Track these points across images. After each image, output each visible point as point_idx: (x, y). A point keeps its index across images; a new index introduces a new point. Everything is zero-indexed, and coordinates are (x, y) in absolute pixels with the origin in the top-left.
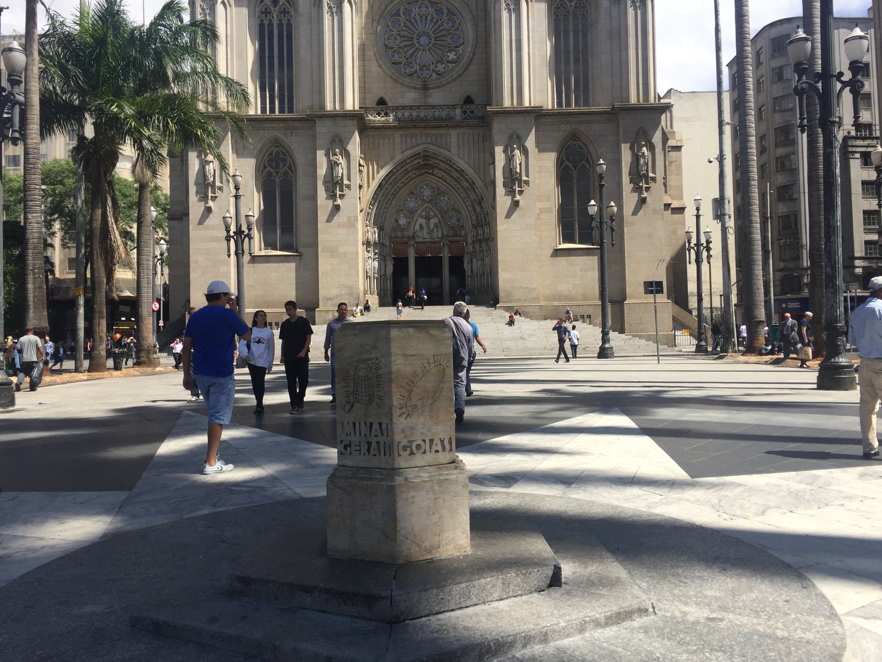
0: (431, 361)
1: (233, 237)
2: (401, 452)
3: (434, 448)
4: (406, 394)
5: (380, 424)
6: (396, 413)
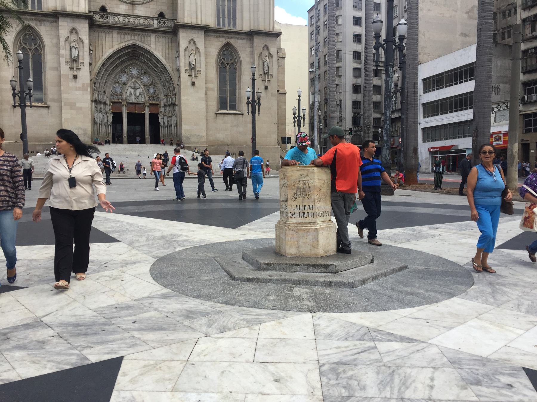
1: (17, 94)
5: (309, 206)
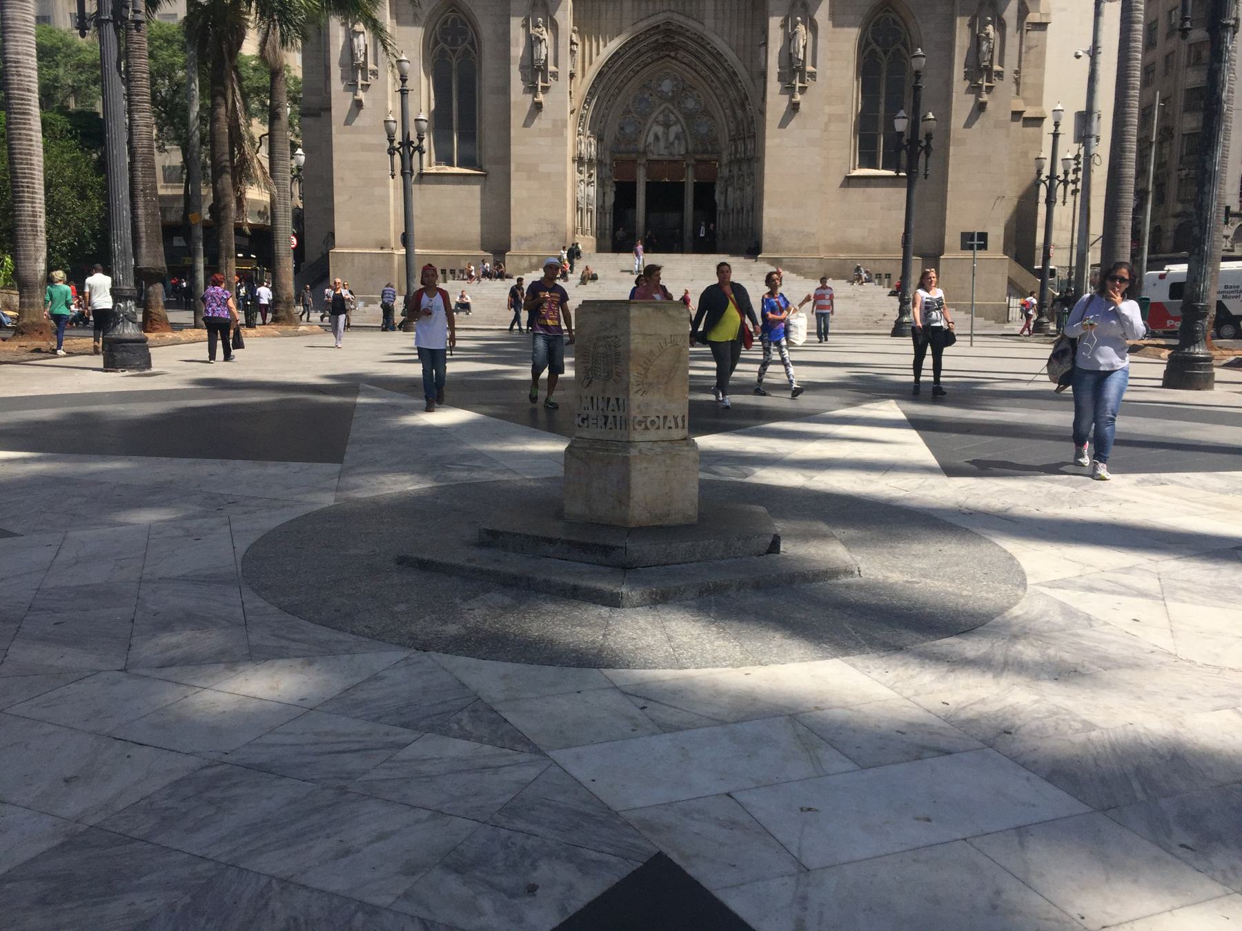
3: (668, 424)
5: (617, 400)
6: (633, 389)
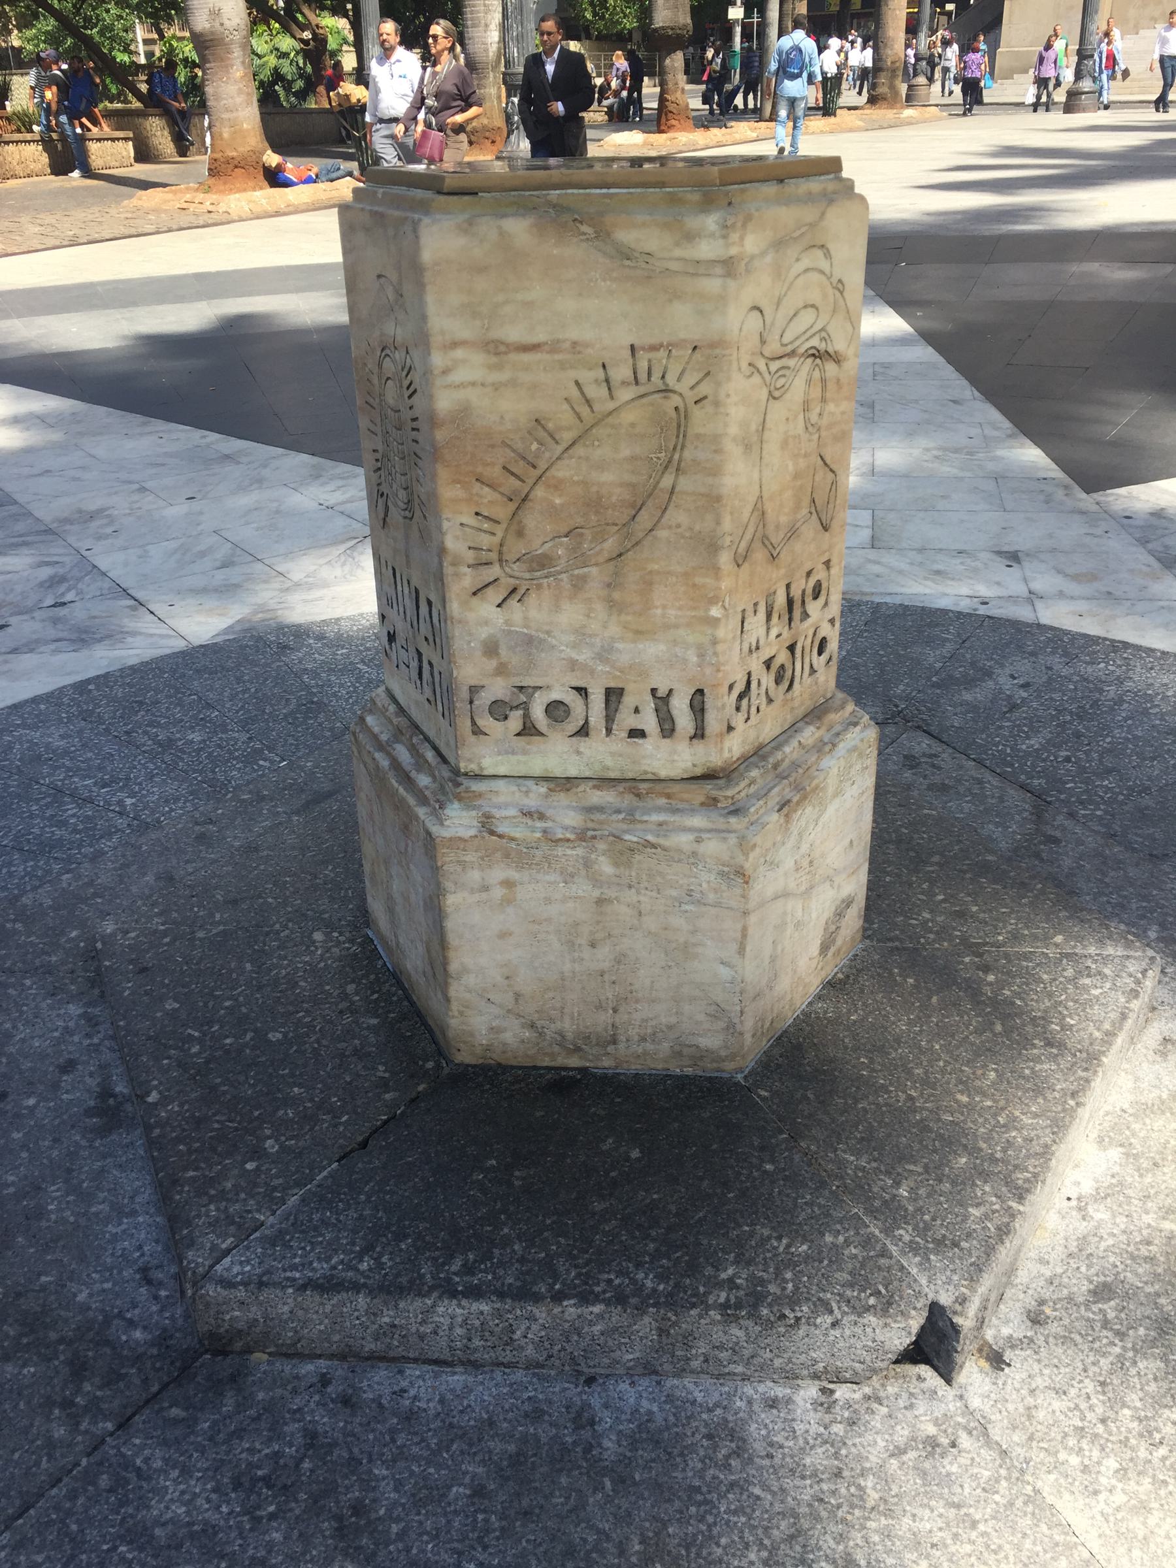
0: (621, 372)
2: (486, 722)
3: (626, 719)
4: (502, 512)
